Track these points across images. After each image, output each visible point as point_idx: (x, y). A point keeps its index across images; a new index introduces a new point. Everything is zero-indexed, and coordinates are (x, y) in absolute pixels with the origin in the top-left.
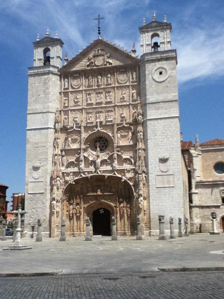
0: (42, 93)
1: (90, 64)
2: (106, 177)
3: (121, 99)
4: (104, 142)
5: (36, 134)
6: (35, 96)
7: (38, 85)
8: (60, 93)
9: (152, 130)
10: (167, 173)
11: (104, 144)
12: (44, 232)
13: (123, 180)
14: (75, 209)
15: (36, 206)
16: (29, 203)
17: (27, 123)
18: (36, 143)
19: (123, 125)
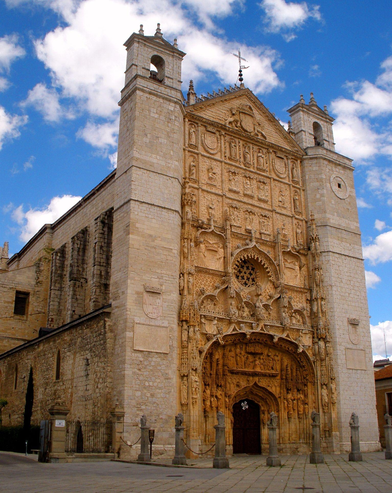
0: (163, 136)
1: (234, 121)
2: (276, 340)
3: (281, 202)
4: (250, 270)
5: (150, 216)
6: (149, 135)
7: (156, 116)
8: (184, 150)
9: (337, 271)
10: (358, 347)
11: (251, 274)
12: (168, 444)
13: (300, 350)
14: (216, 397)
15: (151, 384)
16: (134, 373)
17: (133, 187)
18: (151, 236)
19: (289, 250)
